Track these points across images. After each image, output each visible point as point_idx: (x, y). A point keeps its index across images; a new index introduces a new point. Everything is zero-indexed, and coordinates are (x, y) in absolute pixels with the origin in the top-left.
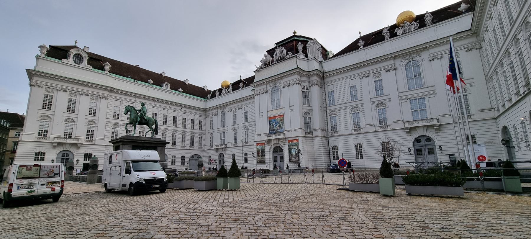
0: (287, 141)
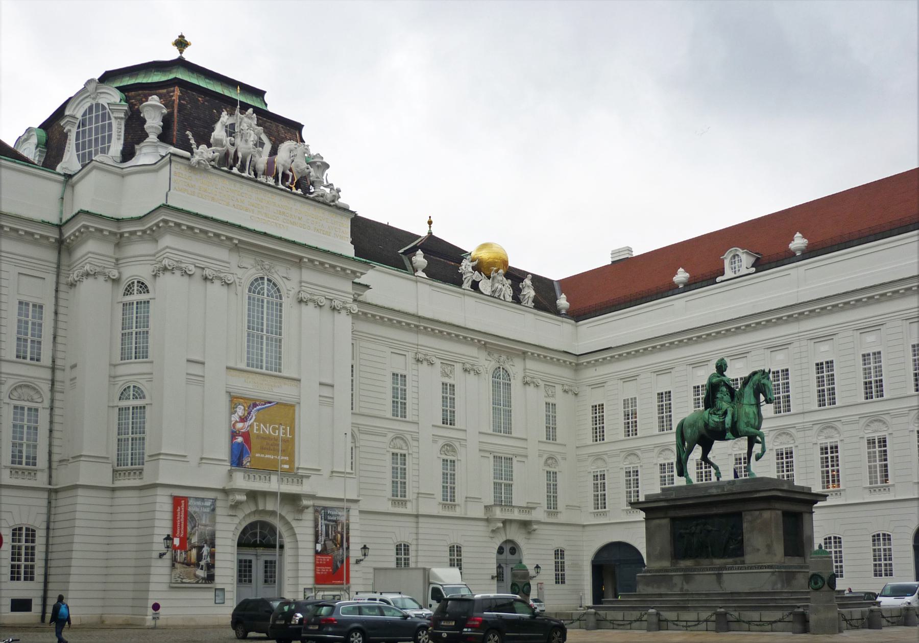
0: (311, 510)
